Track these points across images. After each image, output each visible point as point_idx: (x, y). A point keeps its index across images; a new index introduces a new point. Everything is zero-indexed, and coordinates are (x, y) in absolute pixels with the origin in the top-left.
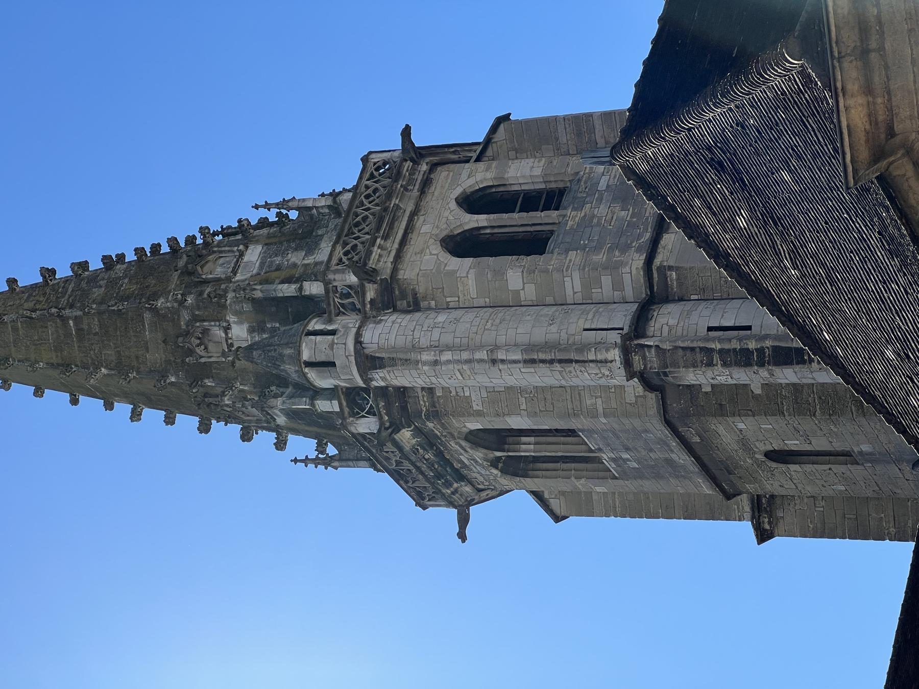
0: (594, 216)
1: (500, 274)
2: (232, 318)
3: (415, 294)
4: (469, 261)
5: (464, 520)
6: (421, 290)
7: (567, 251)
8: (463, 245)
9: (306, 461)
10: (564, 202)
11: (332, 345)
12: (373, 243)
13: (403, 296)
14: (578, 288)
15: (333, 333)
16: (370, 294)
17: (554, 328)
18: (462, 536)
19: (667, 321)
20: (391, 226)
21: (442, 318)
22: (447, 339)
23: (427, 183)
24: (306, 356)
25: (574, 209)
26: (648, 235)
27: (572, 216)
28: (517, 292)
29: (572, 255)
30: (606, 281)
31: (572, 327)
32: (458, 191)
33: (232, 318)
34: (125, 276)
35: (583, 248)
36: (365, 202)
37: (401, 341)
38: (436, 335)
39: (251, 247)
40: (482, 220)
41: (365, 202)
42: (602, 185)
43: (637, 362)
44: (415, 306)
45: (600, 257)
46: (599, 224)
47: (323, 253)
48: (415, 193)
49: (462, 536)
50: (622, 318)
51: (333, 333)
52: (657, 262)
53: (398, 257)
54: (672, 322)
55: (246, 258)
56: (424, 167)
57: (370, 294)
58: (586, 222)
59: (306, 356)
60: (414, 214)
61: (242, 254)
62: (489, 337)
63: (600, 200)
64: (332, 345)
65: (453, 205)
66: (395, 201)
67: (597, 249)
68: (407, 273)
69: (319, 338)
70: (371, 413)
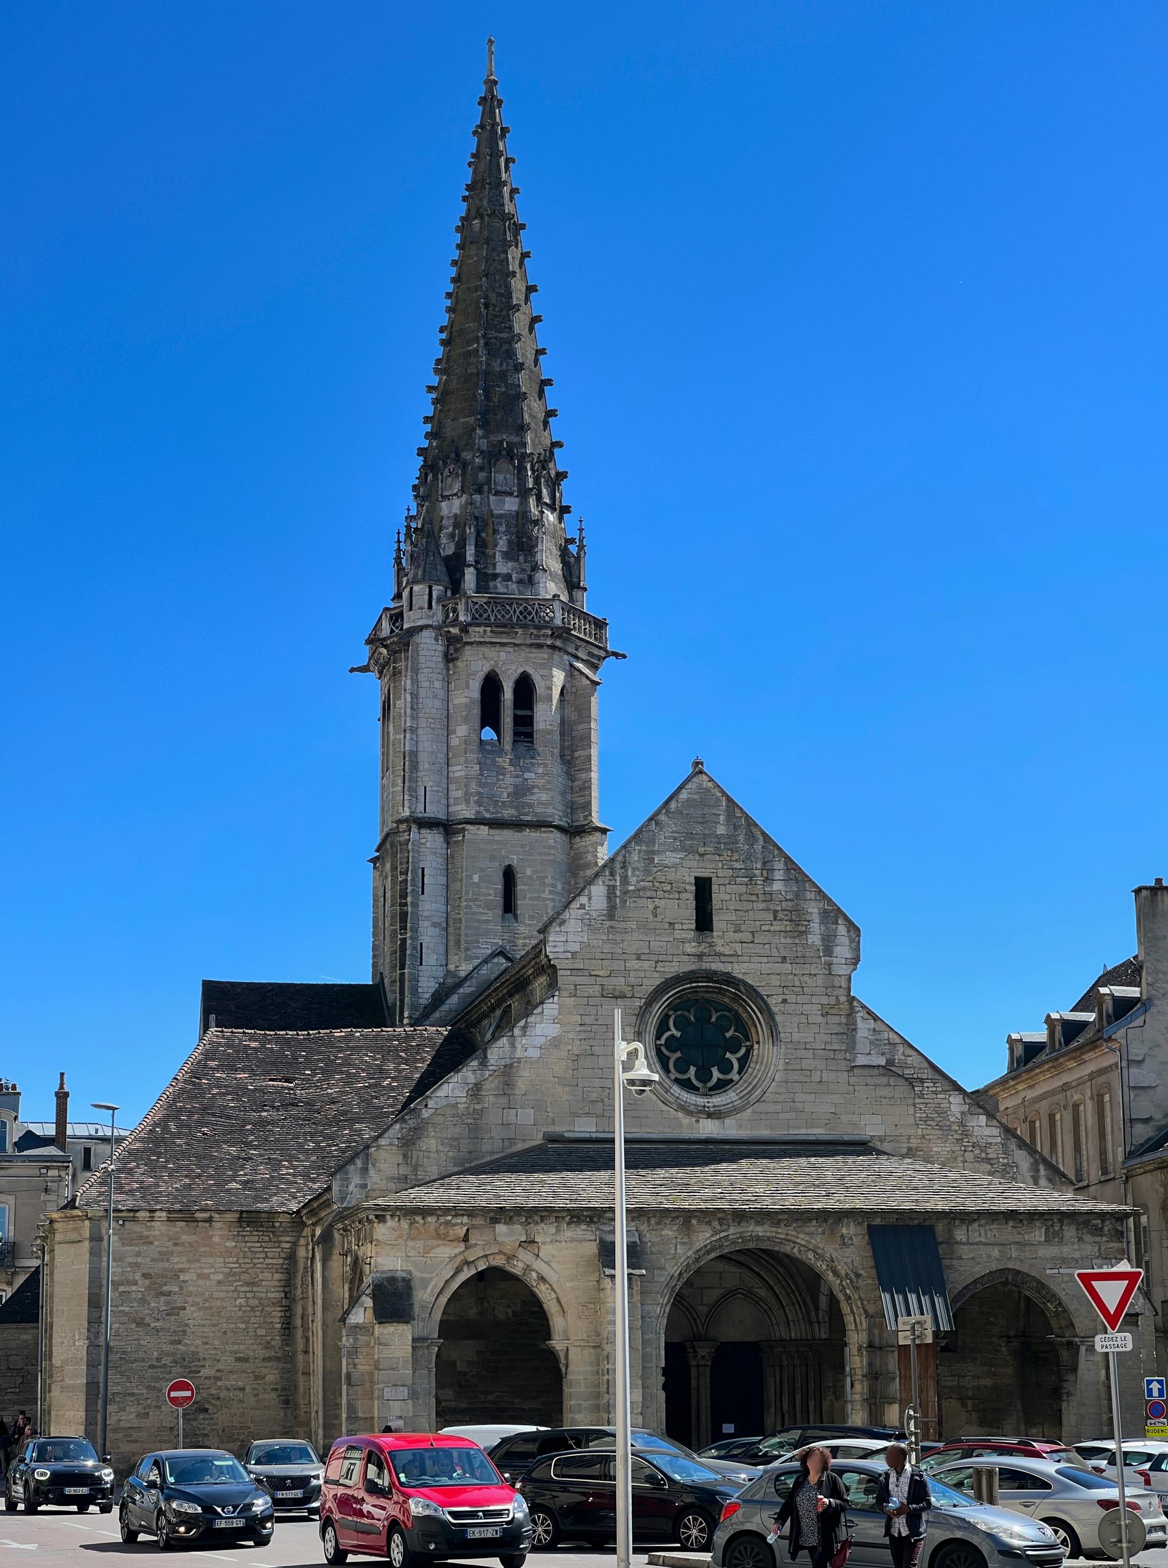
0: (504, 775)
1: (466, 720)
2: (464, 498)
3: (456, 659)
4: (476, 695)
5: (364, 669)
6: (459, 663)
7: (479, 763)
8: (491, 685)
9: (399, 542)
10: (522, 748)
11: (422, 608)
12: (487, 625)
13: (456, 650)
14: (457, 774)
15: (430, 607)
16: (452, 630)
17: (427, 766)
18: (352, 670)
19: (432, 840)
20: (501, 633)
21: (437, 684)
22: (422, 693)
23: (540, 646)
24: (416, 588)
25: (511, 760)
26: (488, 816)
27: (504, 761)
28: (454, 732)
29: (477, 767)
30: (459, 794)
31: (428, 779)
32: (531, 671)
33: (464, 498)
34: (507, 387)
35: (481, 775)
36: (521, 608)
37: (422, 659)
38: (425, 684)
39: (517, 500)
40: (508, 695)
41: (521, 608)
42: (527, 775)
43: (403, 827)
44: (449, 659)
45: (474, 787)
46: (498, 780)
47: (502, 567)
48: (529, 641)
49: (352, 670)
50: (434, 810)
51: (430, 607)
52: (469, 827)
53: (481, 643)
54: (428, 844)
55: (508, 499)
56: (549, 642)
57: (452, 630)
58: (501, 771)
59: (416, 588)
60: (515, 644)
61: (511, 494)
62: (422, 723)
63: (517, 777)
64: (422, 608)
65: (520, 670)
66: (520, 631)
67: (480, 784)
68: (468, 652)
69: (426, 597)
70: (392, 631)
